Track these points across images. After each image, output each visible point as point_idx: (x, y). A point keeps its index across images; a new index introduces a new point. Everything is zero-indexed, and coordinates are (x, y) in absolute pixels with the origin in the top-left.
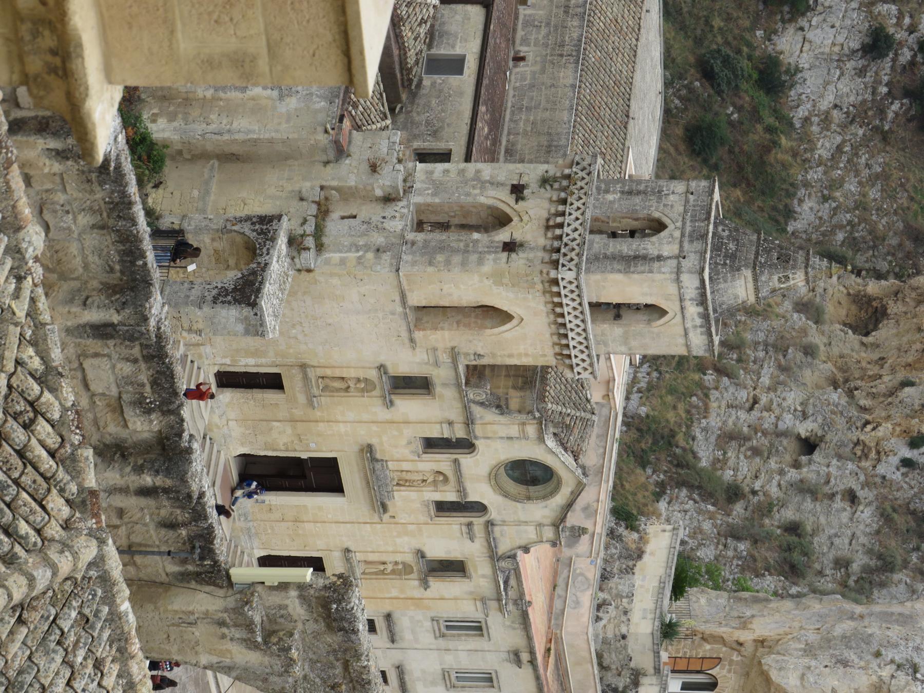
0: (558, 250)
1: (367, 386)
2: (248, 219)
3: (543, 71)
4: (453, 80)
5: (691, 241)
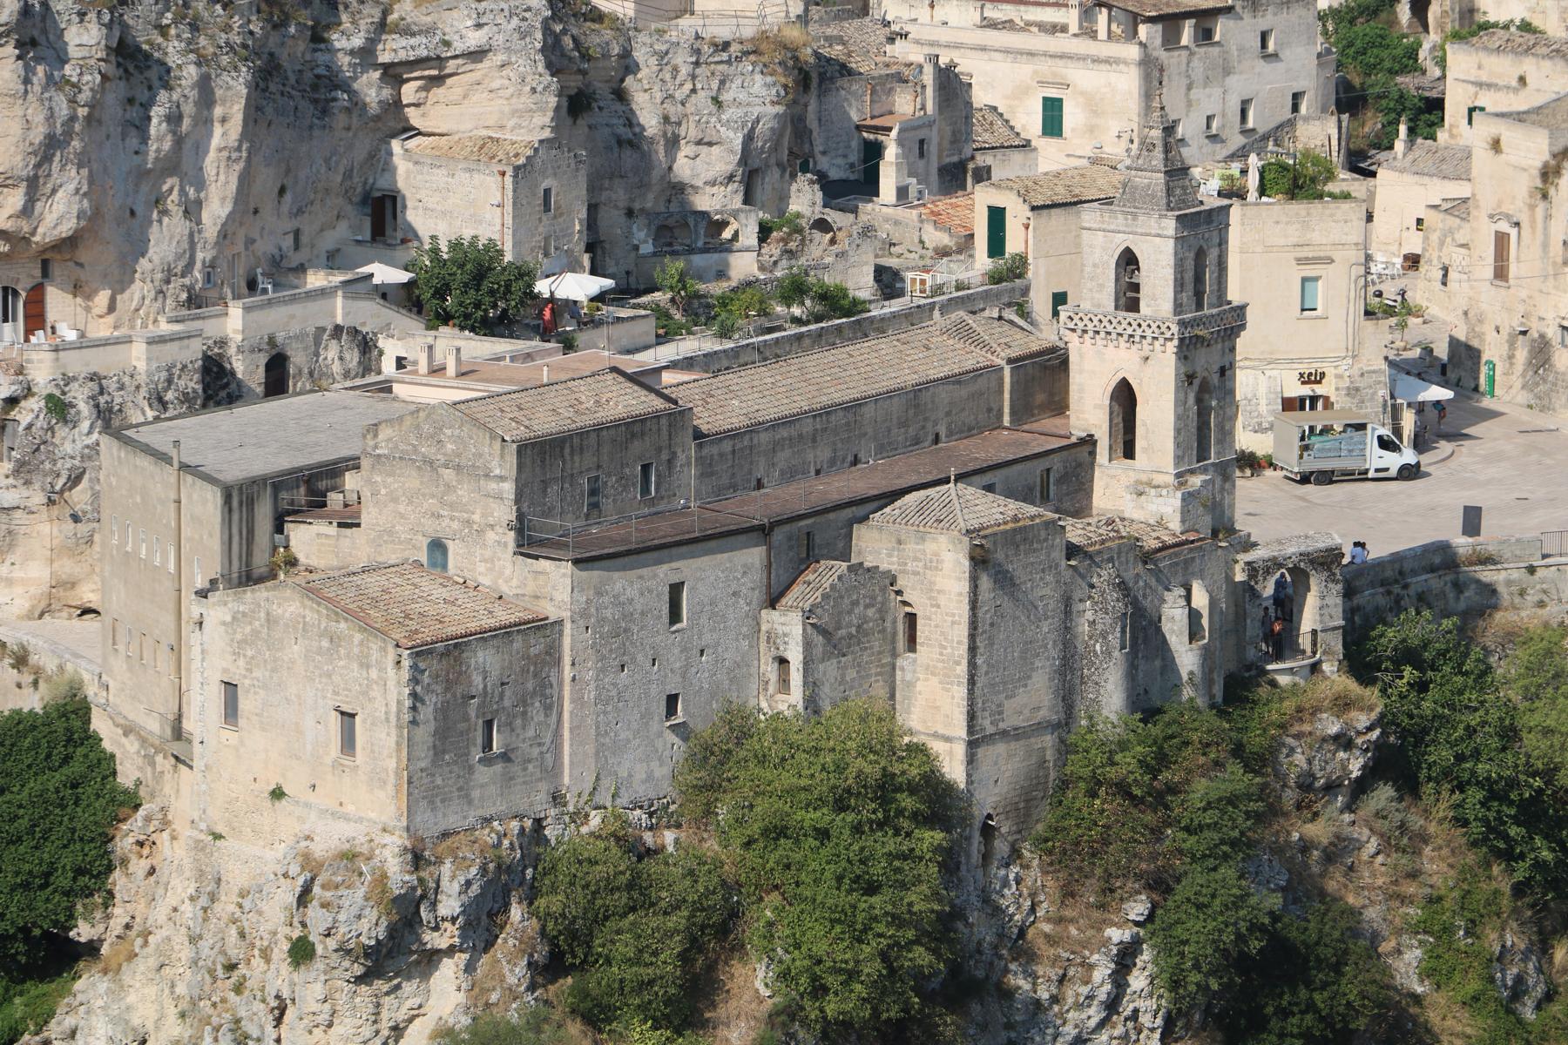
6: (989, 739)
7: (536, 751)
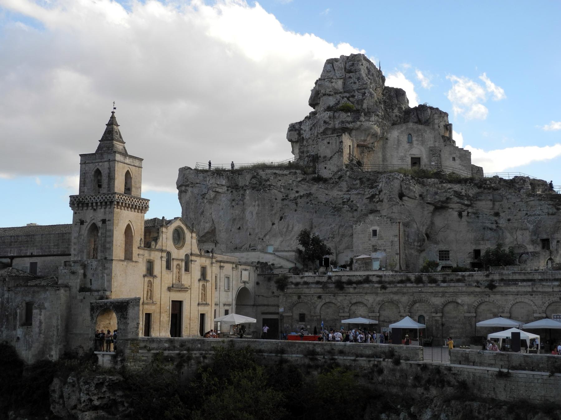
0: (106, 203)
1: (150, 284)
2: (92, 315)
3: (36, 246)
4: (39, 265)
5: (103, 158)
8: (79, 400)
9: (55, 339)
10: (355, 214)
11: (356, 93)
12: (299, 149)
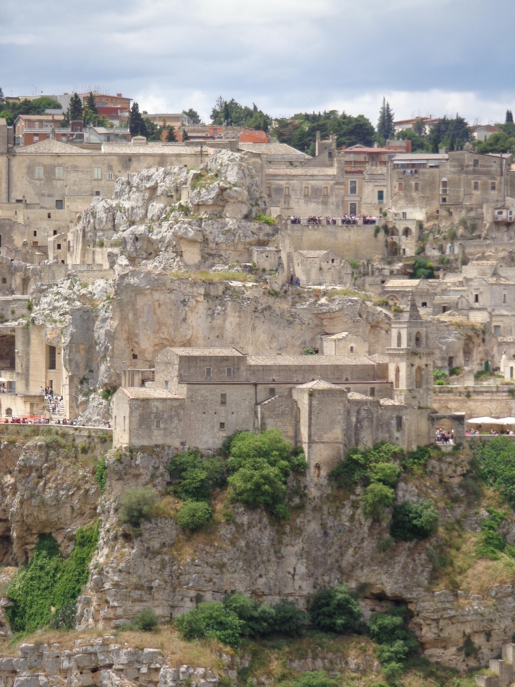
6: (315, 442)
7: (175, 431)
8: (455, 472)
9: (414, 438)
10: (304, 327)
11: (260, 202)
12: (202, 250)
